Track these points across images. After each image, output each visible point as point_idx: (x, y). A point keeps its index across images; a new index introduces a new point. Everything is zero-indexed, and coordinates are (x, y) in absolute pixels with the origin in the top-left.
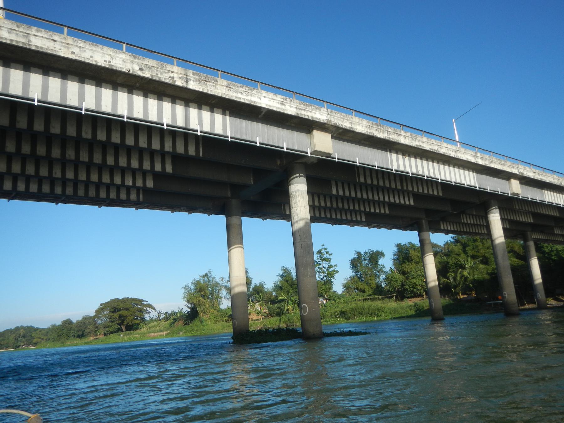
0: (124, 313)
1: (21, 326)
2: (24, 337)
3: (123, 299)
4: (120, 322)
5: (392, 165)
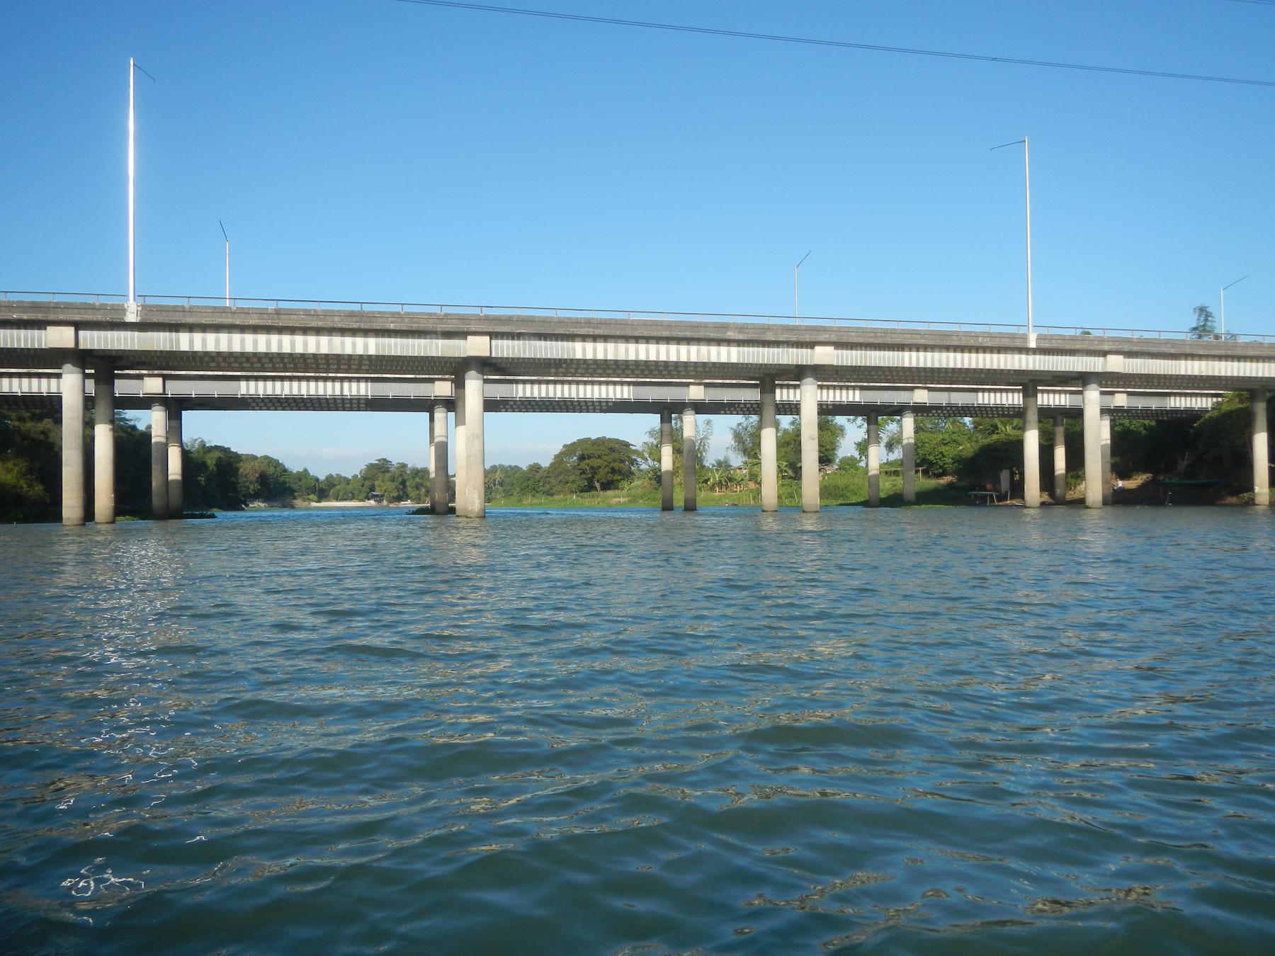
0: (595, 462)
1: (500, 465)
2: (501, 484)
3: (598, 438)
4: (589, 476)
5: (517, 393)
